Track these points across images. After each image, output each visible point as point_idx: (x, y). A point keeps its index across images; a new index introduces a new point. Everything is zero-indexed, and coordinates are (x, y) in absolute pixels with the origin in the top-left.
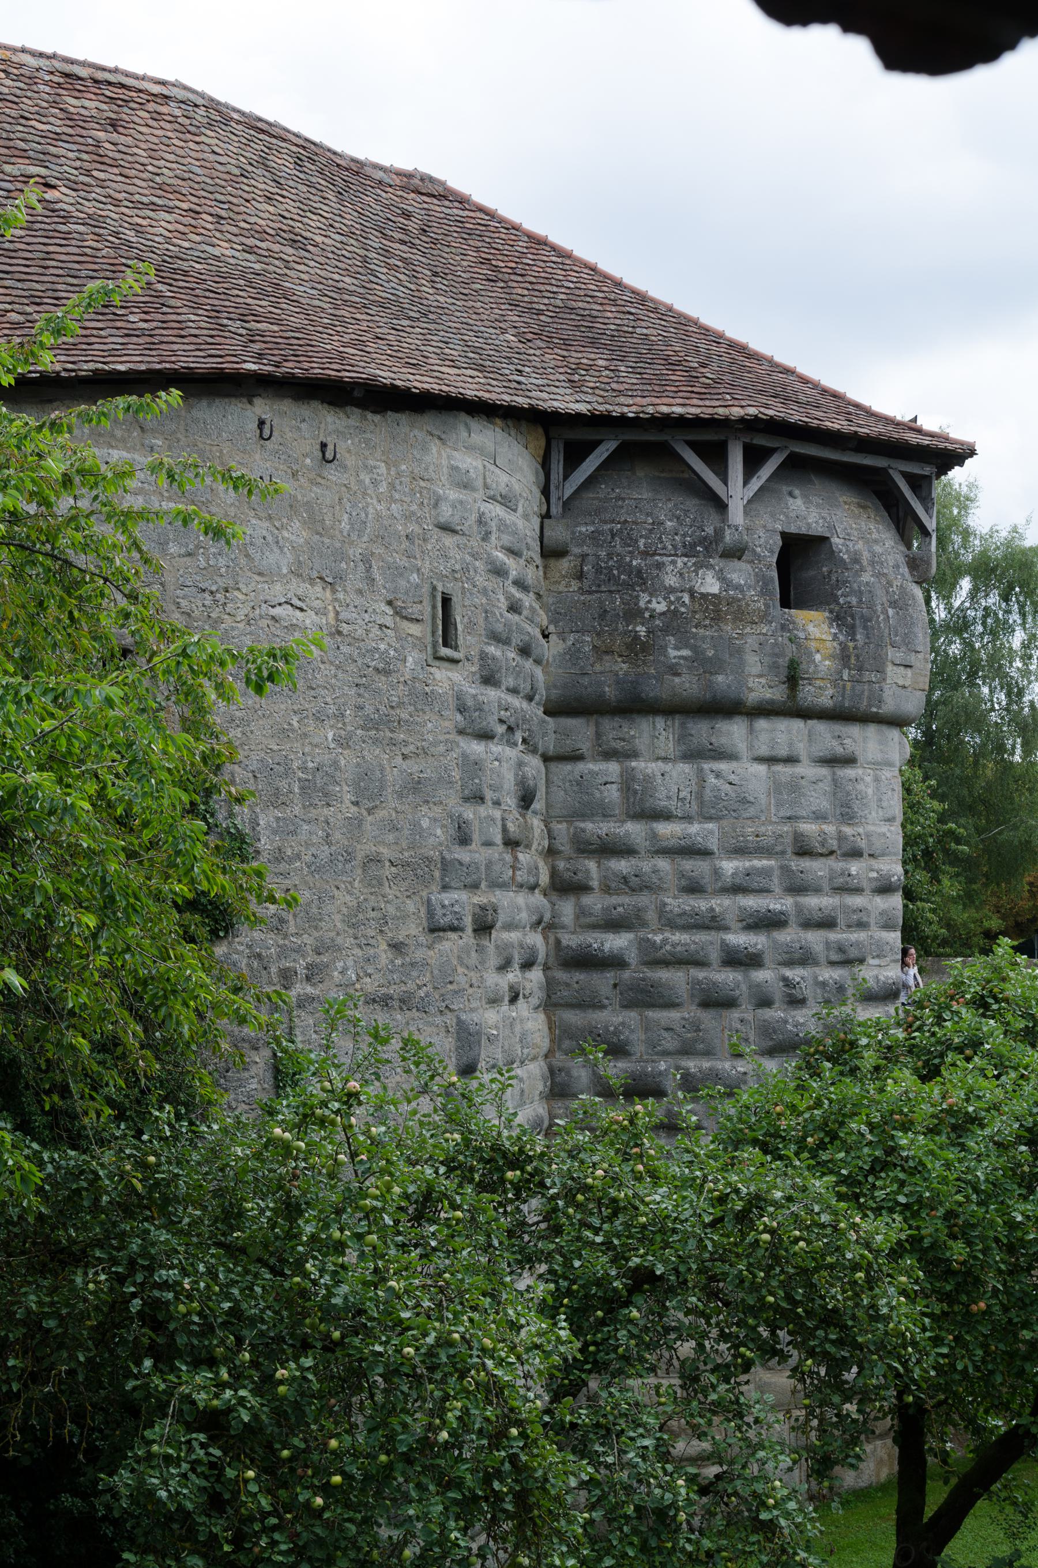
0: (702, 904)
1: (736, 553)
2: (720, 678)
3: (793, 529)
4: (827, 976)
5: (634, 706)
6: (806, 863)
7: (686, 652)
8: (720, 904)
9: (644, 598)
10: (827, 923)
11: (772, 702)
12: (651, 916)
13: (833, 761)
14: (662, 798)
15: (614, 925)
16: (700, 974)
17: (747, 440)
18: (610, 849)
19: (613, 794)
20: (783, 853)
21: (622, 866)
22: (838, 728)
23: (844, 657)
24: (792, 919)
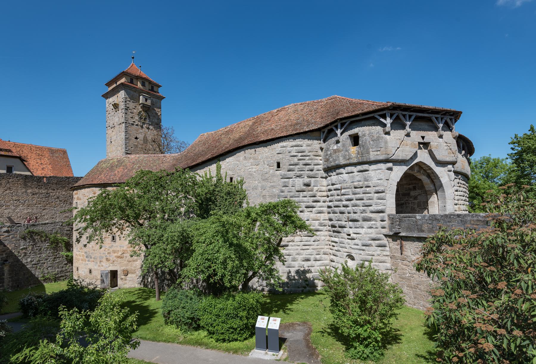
0: (339, 197)
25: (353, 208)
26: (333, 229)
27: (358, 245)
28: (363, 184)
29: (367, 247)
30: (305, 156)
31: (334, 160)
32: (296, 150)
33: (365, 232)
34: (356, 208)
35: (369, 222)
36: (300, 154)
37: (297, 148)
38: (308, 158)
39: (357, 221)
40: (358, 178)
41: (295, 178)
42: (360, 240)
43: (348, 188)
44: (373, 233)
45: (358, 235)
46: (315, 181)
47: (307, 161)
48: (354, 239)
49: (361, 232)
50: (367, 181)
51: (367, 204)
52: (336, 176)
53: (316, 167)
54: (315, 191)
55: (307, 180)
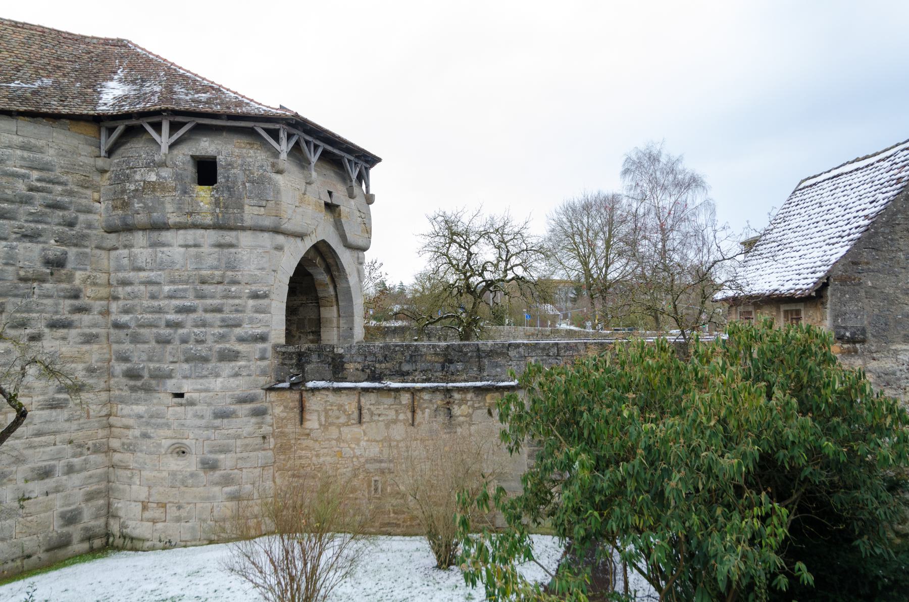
0: (155, 303)
1: (163, 164)
2: (155, 214)
3: (198, 154)
4: (216, 331)
5: (129, 228)
6: (205, 287)
7: (141, 205)
8: (162, 303)
9: (128, 184)
10: (219, 310)
11: (180, 223)
12: (138, 308)
13: (220, 246)
14: (140, 262)
15: (126, 311)
16: (154, 330)
17: (172, 119)
18: (124, 283)
19: (126, 261)
20: (193, 282)
21: (129, 289)
22: (221, 232)
23: (217, 203)
24: (200, 310)
25: (196, 330)
26: (132, 383)
27: (202, 417)
28: (223, 276)
29: (225, 421)
30: (51, 181)
31: (149, 210)
32: (23, 158)
33: (223, 384)
34: (203, 329)
35: (233, 364)
36: (35, 174)
37: (26, 154)
38: (59, 188)
39: (205, 360)
40: (211, 261)
41: (17, 239)
42: (209, 404)
43: (187, 283)
44: (240, 385)
45: (203, 394)
46: (78, 255)
47: (59, 198)
48: (192, 403)
49: (212, 386)
50: (233, 268)
51: (230, 323)
52: (150, 250)
53: (82, 217)
54: (77, 282)
55: (54, 249)
